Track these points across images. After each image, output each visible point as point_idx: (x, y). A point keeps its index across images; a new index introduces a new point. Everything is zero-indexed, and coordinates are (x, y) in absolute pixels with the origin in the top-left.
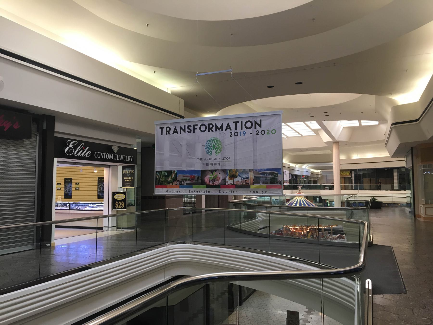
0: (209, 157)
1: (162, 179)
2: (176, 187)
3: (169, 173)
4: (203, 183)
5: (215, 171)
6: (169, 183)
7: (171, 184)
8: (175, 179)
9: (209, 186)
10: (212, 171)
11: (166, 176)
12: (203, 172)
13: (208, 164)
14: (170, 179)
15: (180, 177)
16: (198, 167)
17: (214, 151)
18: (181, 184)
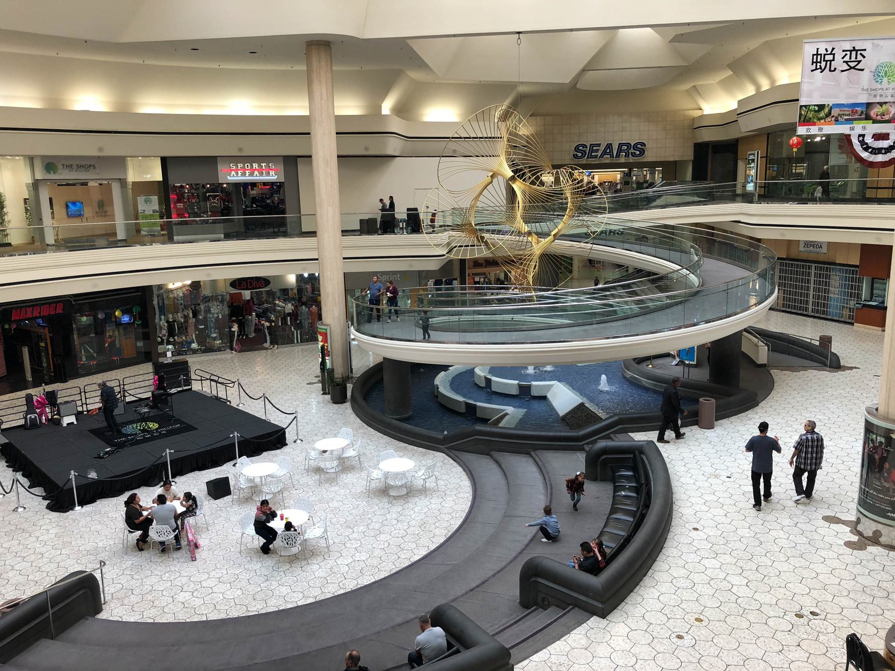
0: (879, 86)
1: (810, 115)
2: (830, 123)
3: (821, 107)
4: (868, 118)
5: (886, 103)
6: (819, 119)
7: (822, 121)
8: (829, 114)
9: (875, 121)
10: (881, 104)
11: (816, 111)
12: (869, 105)
13: (875, 96)
14: (822, 114)
15: (835, 112)
16: (863, 99)
17: (885, 80)
18: (837, 120)
